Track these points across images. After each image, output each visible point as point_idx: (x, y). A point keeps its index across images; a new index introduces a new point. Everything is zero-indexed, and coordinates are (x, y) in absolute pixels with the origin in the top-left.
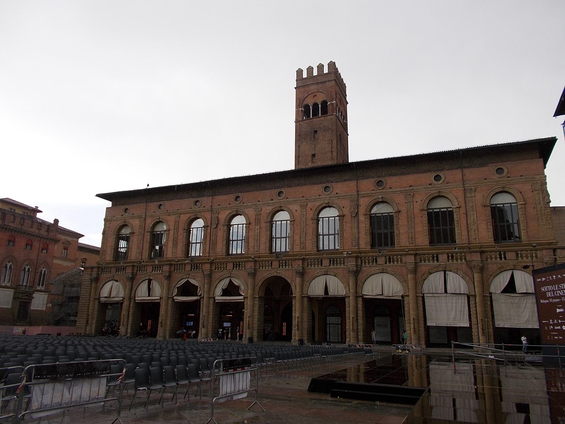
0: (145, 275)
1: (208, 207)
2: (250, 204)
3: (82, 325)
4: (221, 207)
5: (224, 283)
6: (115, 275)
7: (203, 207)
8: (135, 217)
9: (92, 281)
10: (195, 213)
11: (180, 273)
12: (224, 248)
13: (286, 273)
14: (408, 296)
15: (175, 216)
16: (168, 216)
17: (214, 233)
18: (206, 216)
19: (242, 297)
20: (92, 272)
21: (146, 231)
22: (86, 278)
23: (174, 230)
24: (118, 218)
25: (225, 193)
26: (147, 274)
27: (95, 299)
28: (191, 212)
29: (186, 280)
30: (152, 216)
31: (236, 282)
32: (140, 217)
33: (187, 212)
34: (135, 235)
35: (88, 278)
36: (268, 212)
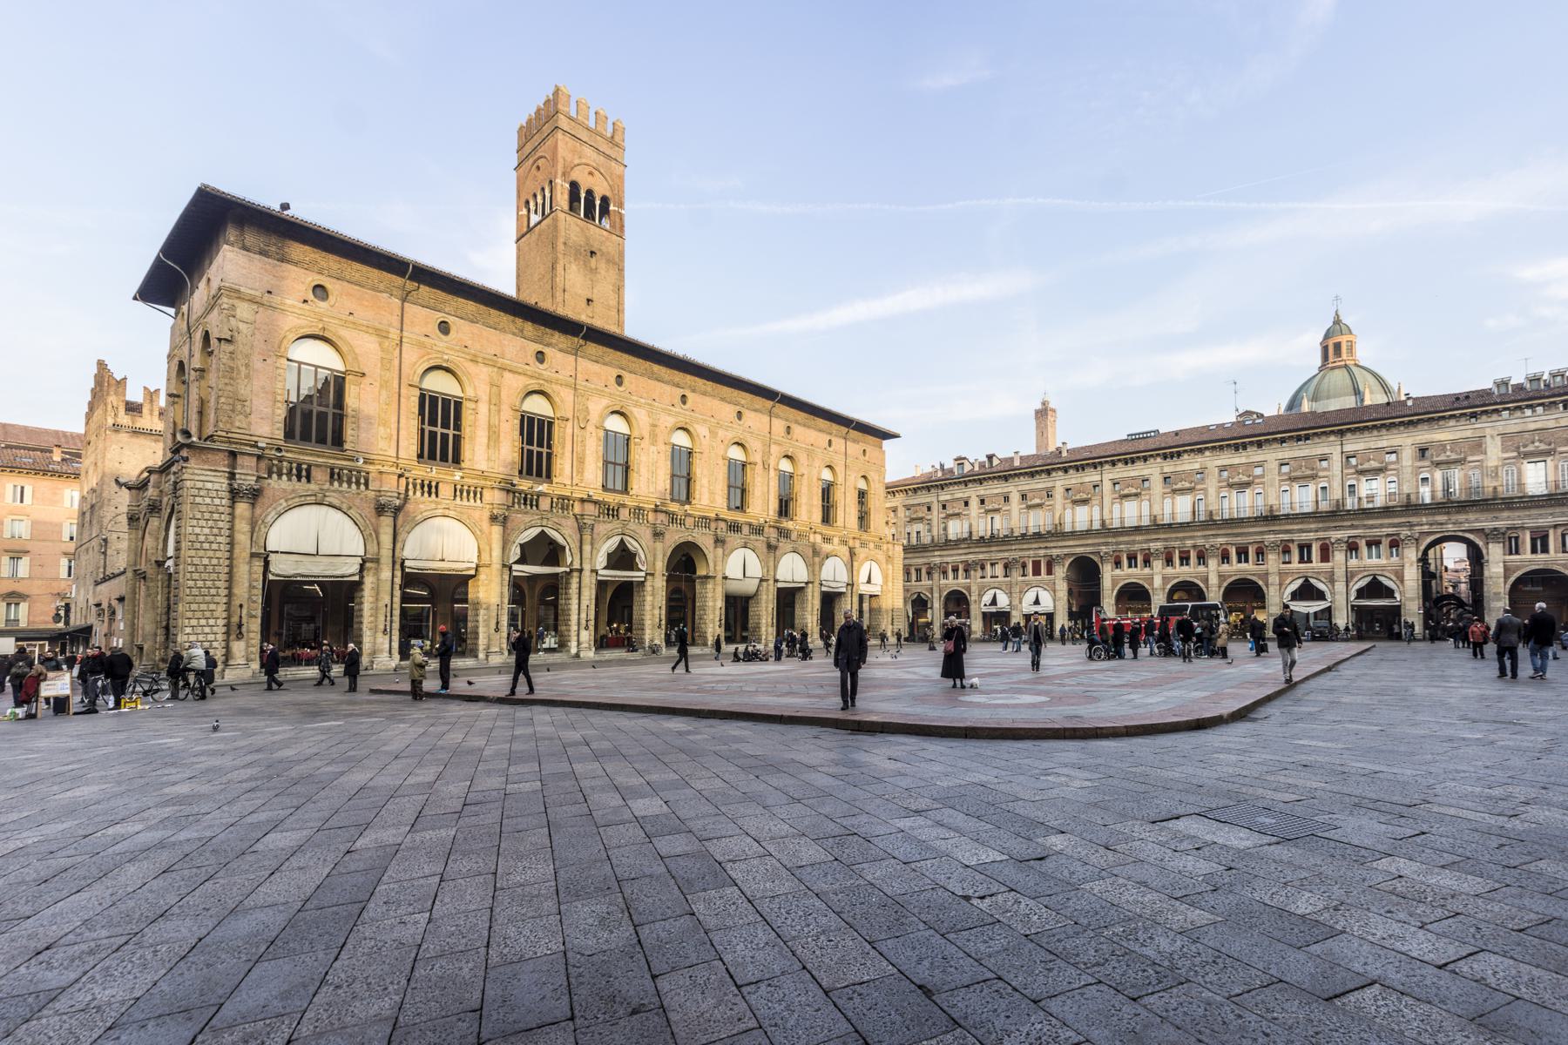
0: (433, 506)
1: (564, 375)
2: (643, 401)
3: (211, 637)
4: (593, 386)
5: (612, 544)
6: (328, 490)
7: (554, 370)
8: (364, 328)
9: (234, 494)
10: (542, 382)
11: (526, 513)
12: (600, 474)
13: (704, 540)
14: (812, 583)
15: (490, 369)
16: (471, 363)
17: (580, 439)
18: (562, 394)
19: (643, 574)
20: (233, 465)
21: (405, 382)
22: (209, 485)
23: (490, 404)
24: (294, 307)
25: (594, 358)
26: (437, 503)
27: (253, 555)
28: (528, 373)
29: (540, 529)
30: (421, 345)
31: (632, 545)
32: (382, 334)
33: (520, 371)
34: (366, 380)
35: (217, 486)
36: (669, 425)
